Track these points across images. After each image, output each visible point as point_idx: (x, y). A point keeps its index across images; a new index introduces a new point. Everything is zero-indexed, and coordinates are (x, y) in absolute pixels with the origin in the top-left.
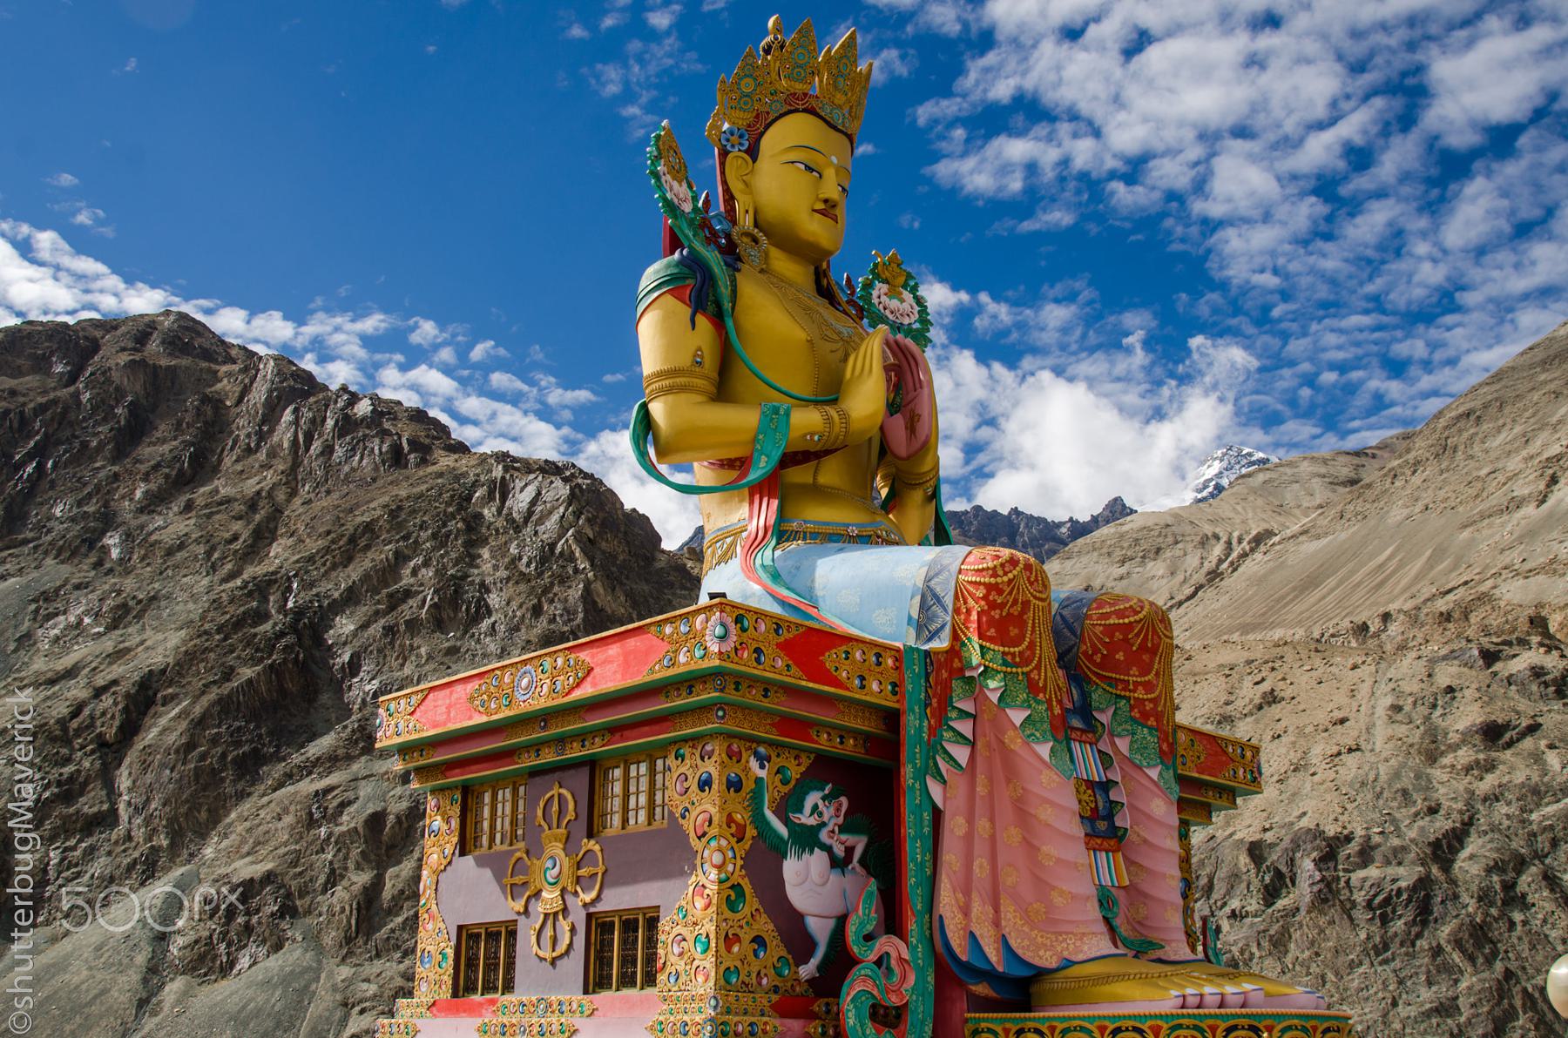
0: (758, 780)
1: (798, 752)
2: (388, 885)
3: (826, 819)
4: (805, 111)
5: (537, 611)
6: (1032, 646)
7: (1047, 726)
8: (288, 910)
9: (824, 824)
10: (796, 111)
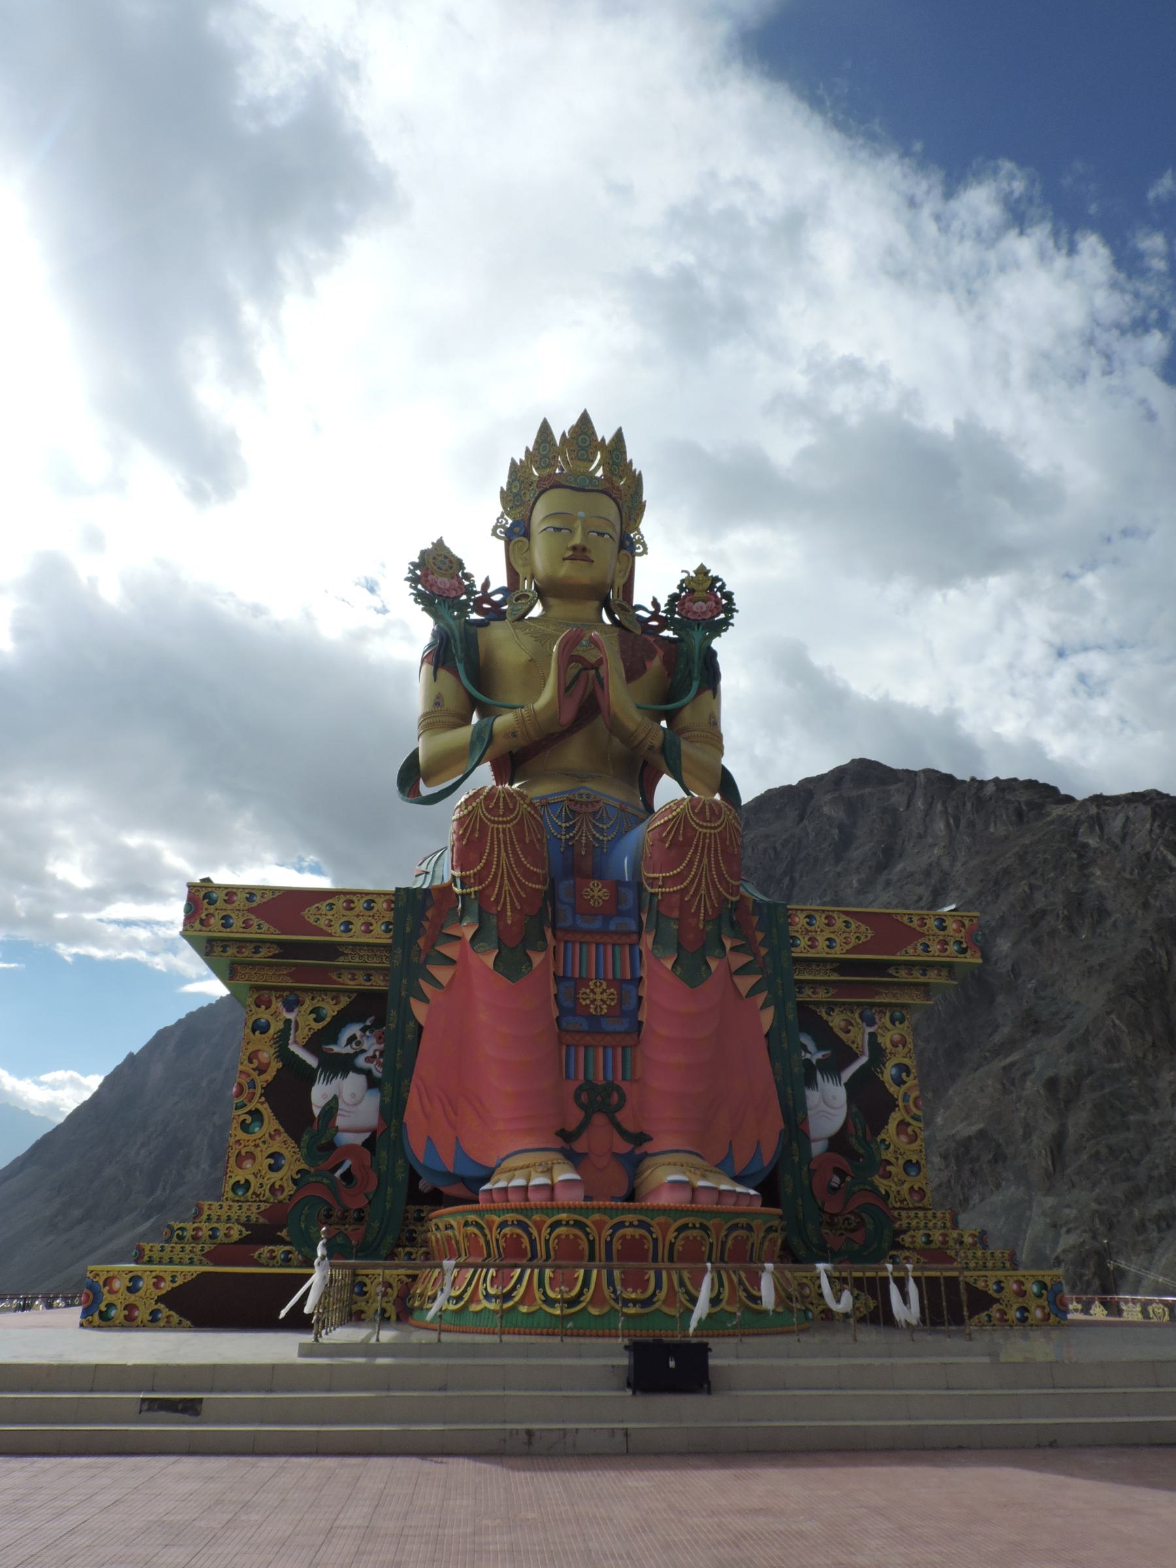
0: (288, 1022)
1: (336, 994)
2: (1071, 1130)
3: (365, 1047)
4: (552, 487)
5: (1146, 906)
6: (489, 864)
8: (999, 1157)
9: (363, 1051)
10: (545, 490)
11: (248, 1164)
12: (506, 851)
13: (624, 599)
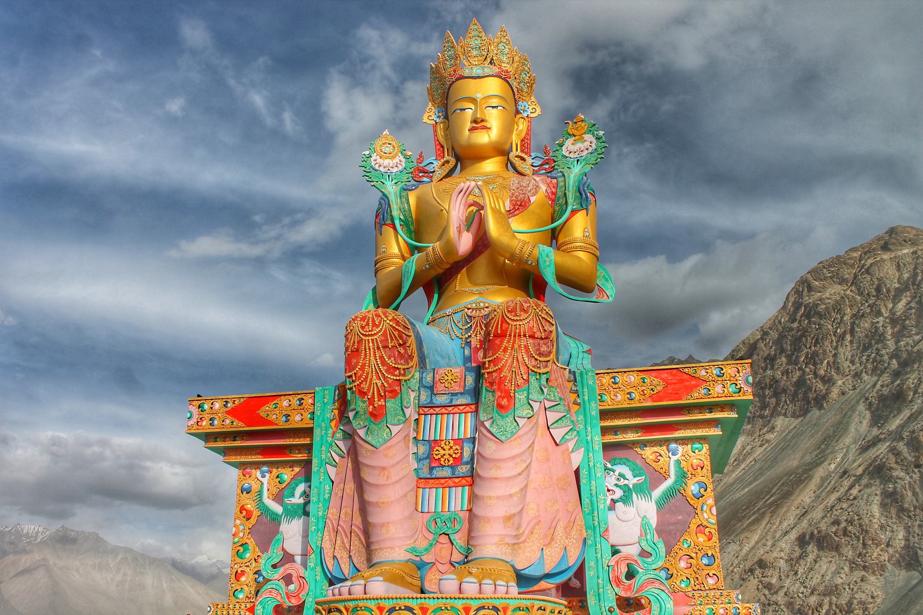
1: (292, 464)
6: (363, 366)
7: (368, 416)
10: (453, 82)
11: (243, 579)
12: (375, 355)
13: (522, 151)
